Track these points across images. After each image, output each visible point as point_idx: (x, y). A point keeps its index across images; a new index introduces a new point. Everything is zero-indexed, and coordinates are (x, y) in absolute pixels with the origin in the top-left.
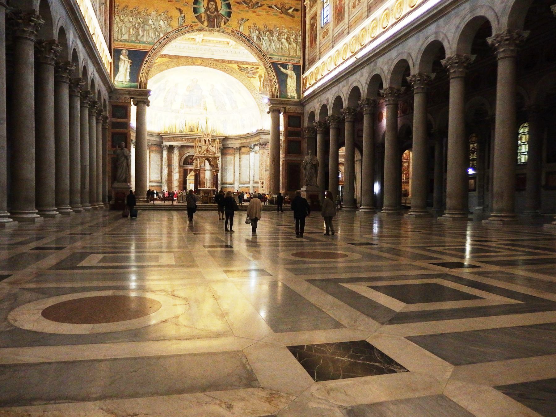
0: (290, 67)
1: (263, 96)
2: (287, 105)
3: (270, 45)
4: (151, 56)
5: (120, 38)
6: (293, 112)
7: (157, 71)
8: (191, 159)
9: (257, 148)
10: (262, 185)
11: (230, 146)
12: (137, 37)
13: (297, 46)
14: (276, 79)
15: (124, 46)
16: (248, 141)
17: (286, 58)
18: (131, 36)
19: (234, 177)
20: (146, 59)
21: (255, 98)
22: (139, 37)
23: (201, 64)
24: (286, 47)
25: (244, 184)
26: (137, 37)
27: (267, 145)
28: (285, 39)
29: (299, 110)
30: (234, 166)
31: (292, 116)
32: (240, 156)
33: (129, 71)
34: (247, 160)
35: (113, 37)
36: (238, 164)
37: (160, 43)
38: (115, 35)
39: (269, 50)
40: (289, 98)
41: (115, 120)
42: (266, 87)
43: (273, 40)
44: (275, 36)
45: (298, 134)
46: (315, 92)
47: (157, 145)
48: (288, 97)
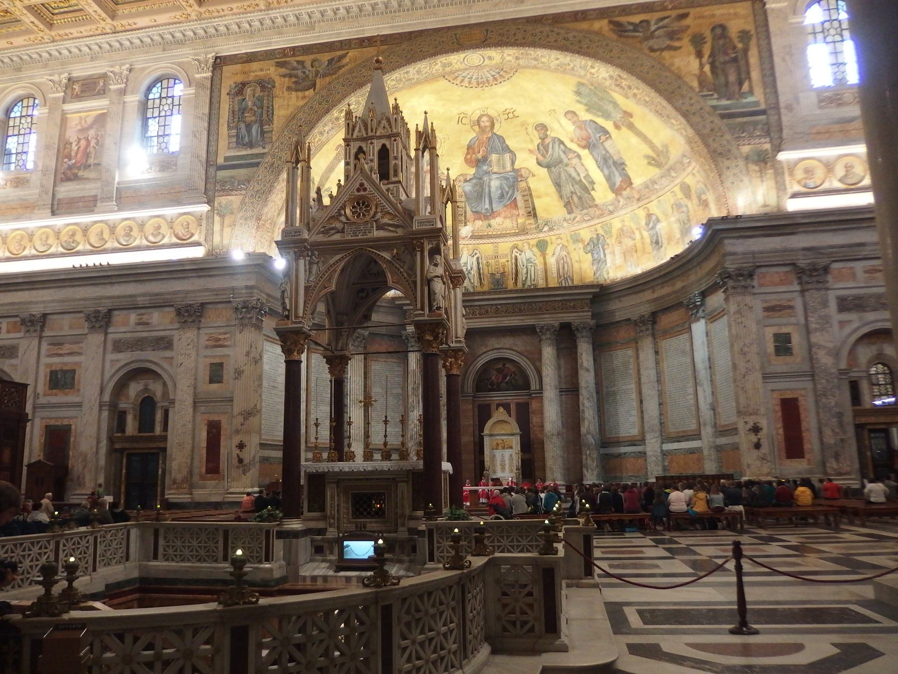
1: (714, 103)
8: (499, 371)
9: (716, 300)
10: (754, 438)
11: (619, 316)
16: (679, 285)
19: (642, 418)
21: (685, 115)
25: (679, 439)
27: (756, 277)
30: (639, 379)
32: (655, 344)
34: (683, 352)
36: (653, 373)
42: (723, 71)
47: (392, 336)
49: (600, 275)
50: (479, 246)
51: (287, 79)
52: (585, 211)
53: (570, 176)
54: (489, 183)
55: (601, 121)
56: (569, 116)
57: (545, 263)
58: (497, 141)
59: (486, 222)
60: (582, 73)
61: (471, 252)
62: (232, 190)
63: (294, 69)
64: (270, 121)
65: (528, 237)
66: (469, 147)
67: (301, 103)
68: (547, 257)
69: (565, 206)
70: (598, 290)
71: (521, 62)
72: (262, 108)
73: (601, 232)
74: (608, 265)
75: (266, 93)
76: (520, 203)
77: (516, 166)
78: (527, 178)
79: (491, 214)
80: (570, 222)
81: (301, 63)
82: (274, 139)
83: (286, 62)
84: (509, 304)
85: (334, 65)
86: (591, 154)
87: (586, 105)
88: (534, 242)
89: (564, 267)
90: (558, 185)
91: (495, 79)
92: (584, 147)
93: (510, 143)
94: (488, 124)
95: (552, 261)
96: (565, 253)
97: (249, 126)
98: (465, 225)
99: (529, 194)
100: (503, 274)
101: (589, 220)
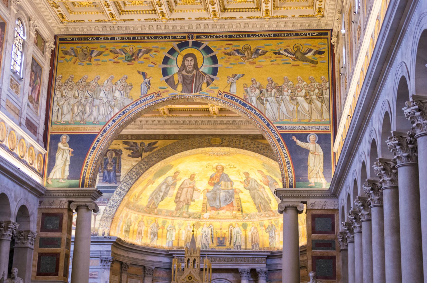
0: (312, 137)
2: (308, 197)
3: (279, 108)
4: (100, 141)
5: (59, 120)
6: (320, 208)
7: (156, 159)
12: (83, 116)
13: (322, 106)
14: (289, 159)
15: (65, 130)
17: (305, 125)
18: (75, 115)
20: (94, 145)
22: (86, 116)
23: (221, 145)
24: (304, 109)
26: (83, 116)
28: (302, 97)
29: (330, 204)
31: (320, 216)
33: (68, 163)
35: (51, 119)
37: (114, 121)
38: (54, 117)
39: (277, 116)
40: (311, 187)
41: (44, 235)
43: (283, 100)
44: (287, 94)
45: (329, 245)
46: (336, 175)
48: (311, 185)
49: (272, 245)
50: (213, 223)
51: (128, 151)
52: (266, 212)
53: (260, 195)
54: (220, 193)
55: (274, 177)
56: (259, 171)
57: (246, 235)
58: (225, 176)
59: (217, 212)
60: (265, 160)
61: (208, 225)
62: (100, 203)
63: (132, 146)
64: (120, 171)
65: (238, 221)
66: (211, 178)
67: (134, 164)
68: (247, 231)
69: (257, 208)
70: (269, 254)
71: (238, 152)
72: (116, 164)
73: (274, 223)
74: (276, 240)
75: (118, 157)
76: (235, 204)
77: (234, 187)
78: (239, 193)
79: (219, 208)
80: (259, 216)
81: (135, 143)
82: (121, 180)
83: (128, 142)
84: (226, 257)
85: (150, 147)
86: (270, 188)
87: (267, 170)
88: (240, 223)
89: (255, 238)
90: (254, 198)
91: (225, 154)
92: (266, 185)
93: (232, 178)
94: (221, 169)
95: (249, 234)
96: (256, 231)
97: (109, 172)
98: (206, 212)
99: (239, 201)
100: (224, 238)
101: (268, 217)
